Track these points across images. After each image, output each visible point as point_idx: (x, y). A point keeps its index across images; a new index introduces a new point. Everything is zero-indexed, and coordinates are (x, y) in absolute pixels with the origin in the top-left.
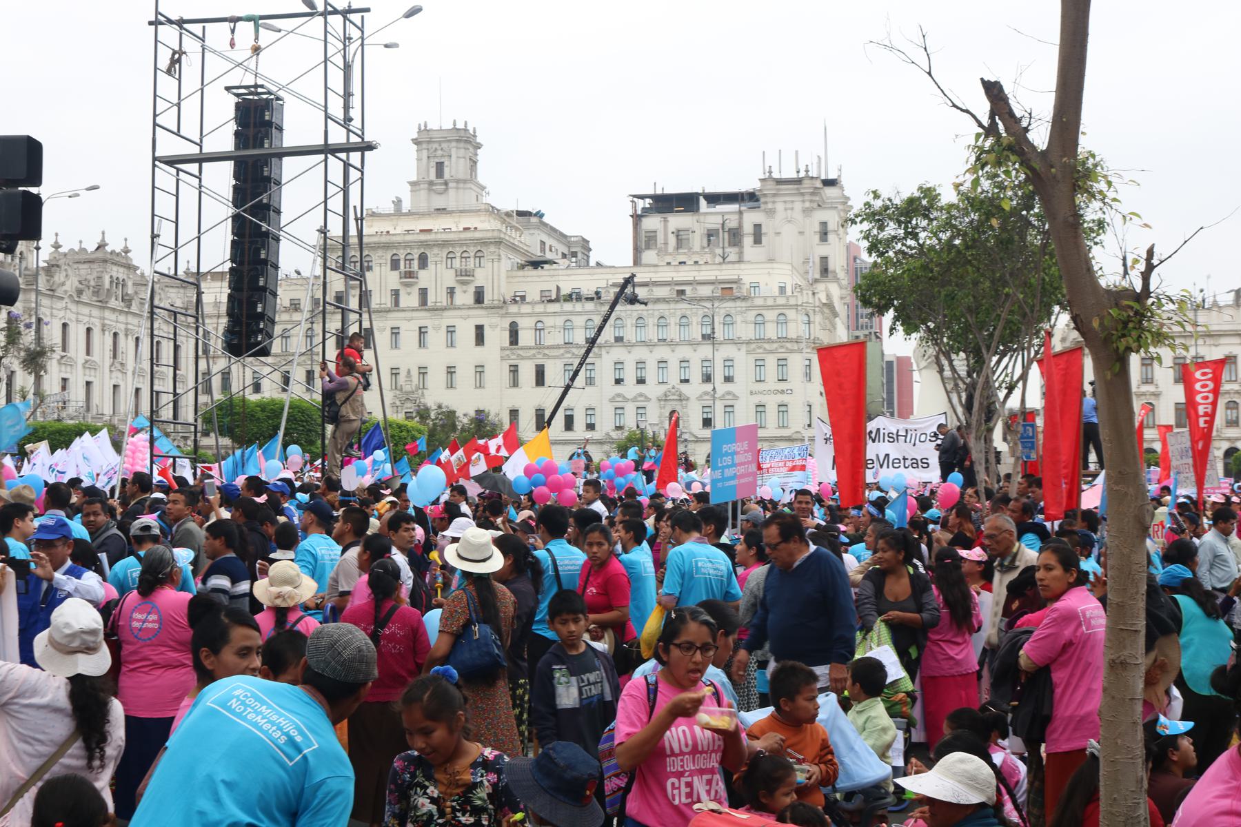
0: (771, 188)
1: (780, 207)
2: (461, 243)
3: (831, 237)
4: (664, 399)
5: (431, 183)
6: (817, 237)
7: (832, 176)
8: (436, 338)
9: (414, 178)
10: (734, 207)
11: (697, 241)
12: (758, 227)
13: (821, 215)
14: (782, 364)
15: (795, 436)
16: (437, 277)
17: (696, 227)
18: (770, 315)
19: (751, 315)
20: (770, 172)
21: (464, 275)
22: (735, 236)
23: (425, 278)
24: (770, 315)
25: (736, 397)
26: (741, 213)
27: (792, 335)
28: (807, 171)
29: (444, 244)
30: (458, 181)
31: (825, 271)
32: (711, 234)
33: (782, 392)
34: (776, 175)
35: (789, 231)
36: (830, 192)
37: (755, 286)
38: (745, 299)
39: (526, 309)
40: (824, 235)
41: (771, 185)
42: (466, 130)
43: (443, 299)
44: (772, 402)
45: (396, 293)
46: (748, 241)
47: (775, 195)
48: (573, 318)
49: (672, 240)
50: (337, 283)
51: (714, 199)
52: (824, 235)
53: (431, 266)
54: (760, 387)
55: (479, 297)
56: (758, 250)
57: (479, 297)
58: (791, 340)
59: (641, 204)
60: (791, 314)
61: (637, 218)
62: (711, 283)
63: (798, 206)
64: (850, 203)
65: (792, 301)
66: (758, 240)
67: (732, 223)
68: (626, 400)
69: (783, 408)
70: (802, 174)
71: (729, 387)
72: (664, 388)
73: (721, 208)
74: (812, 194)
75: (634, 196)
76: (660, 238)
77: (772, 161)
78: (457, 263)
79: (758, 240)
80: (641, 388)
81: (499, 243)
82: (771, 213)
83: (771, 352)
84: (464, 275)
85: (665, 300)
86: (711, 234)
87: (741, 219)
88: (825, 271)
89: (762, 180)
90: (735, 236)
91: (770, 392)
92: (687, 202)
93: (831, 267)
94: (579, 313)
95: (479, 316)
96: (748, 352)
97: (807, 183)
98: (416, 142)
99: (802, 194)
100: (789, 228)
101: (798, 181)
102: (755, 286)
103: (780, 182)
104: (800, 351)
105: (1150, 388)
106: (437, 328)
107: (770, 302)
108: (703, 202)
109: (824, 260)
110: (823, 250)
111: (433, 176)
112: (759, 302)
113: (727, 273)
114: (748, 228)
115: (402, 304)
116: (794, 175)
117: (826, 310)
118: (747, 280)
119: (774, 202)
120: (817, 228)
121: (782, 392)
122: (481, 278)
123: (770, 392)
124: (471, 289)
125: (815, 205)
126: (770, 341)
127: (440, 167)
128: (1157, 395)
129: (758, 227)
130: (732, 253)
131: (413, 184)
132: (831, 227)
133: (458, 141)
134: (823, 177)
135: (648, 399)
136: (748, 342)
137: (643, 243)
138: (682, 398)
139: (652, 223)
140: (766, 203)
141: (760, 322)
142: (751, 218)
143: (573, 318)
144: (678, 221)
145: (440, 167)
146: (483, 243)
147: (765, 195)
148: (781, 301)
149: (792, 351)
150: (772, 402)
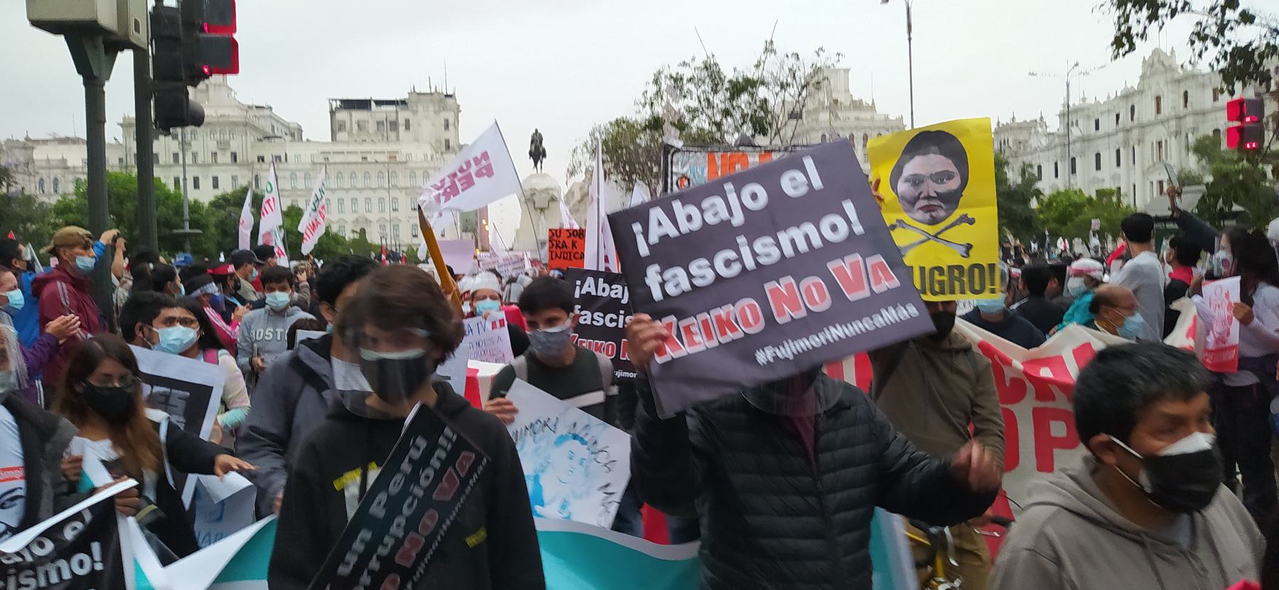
0: (414, 97)
1: (420, 109)
2: (219, 124)
3: (451, 127)
4: (357, 221)
7: (450, 93)
10: (392, 108)
11: (372, 127)
12: (407, 122)
13: (445, 115)
21: (223, 145)
22: (394, 125)
31: (448, 147)
32: (379, 123)
34: (417, 90)
36: (449, 101)
37: (409, 155)
40: (447, 126)
45: (176, 156)
46: (402, 128)
49: (355, 126)
51: (379, 103)
52: (447, 126)
55: (234, 157)
56: (407, 133)
57: (234, 157)
61: (332, 113)
63: (431, 109)
66: (407, 127)
67: (393, 118)
71: (394, 214)
73: (384, 108)
76: (348, 125)
78: (217, 137)
79: (407, 127)
80: (342, 216)
81: (246, 124)
82: (415, 112)
84: (223, 145)
85: (356, 163)
86: (379, 123)
88: (448, 147)
90: (394, 125)
92: (363, 105)
95: (235, 170)
100: (426, 123)
102: (409, 155)
106: (206, 177)
109: (447, 142)
110: (447, 135)
112: (411, 165)
113: (392, 147)
114: (401, 121)
118: (404, 152)
122: (235, 145)
129: (407, 122)
130: (392, 135)
132: (451, 121)
137: (337, 128)
138: (367, 221)
139: (343, 115)
141: (413, 175)
142: (403, 115)
144: (358, 115)
146: (235, 124)
148: (426, 165)
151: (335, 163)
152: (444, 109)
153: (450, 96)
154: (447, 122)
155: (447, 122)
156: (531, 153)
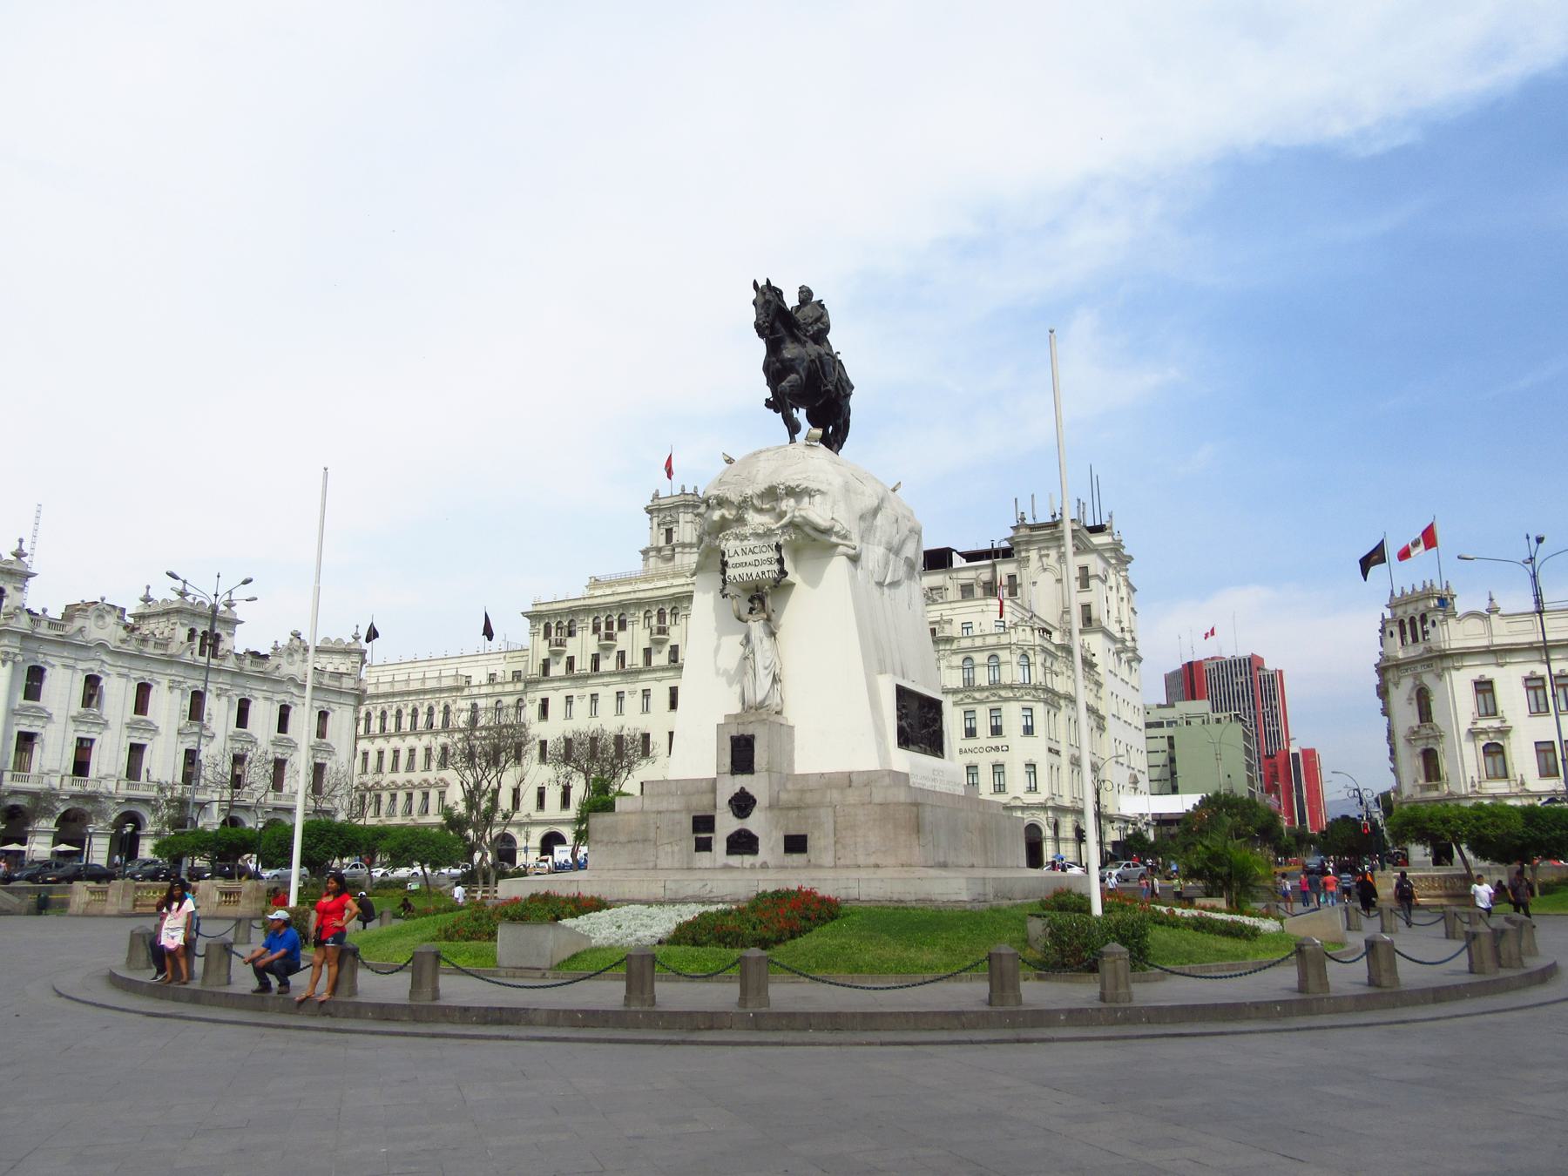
1: (1034, 555)
3: (1093, 583)
5: (659, 550)
6: (1076, 585)
8: (633, 703)
9: (647, 544)
11: (953, 593)
12: (1012, 577)
14: (995, 713)
16: (633, 640)
17: (949, 584)
18: (981, 658)
19: (957, 660)
20: (1023, 519)
23: (622, 640)
24: (981, 658)
26: (994, 566)
27: (1006, 680)
29: (638, 604)
30: (684, 545)
31: (1088, 619)
33: (997, 749)
34: (1029, 521)
36: (1097, 539)
37: (967, 626)
41: (1024, 532)
42: (695, 494)
43: (639, 662)
44: (985, 762)
47: (1028, 543)
50: (543, 649)
51: (971, 556)
52: (1085, 578)
53: (629, 627)
54: (971, 743)
58: (1005, 687)
60: (1004, 655)
64: (1125, 552)
65: (1004, 640)
66: (1013, 593)
69: (998, 768)
77: (1025, 507)
79: (1013, 593)
83: (981, 702)
87: (994, 571)
91: (981, 750)
93: (1094, 615)
96: (955, 704)
98: (649, 511)
102: (967, 626)
103: (1033, 528)
104: (1016, 699)
105: (1495, 723)
107: (978, 642)
108: (958, 561)
109: (1086, 608)
110: (1085, 597)
111: (662, 543)
112: (966, 643)
115: (602, 668)
116: (1050, 520)
119: (1027, 550)
121: (997, 749)
123: (981, 750)
124: (667, 649)
126: (981, 689)
127: (669, 532)
128: (1504, 732)
131: (645, 553)
132: (1091, 572)
133: (686, 506)
134: (1090, 524)
142: (1005, 569)
145: (669, 532)
147: (1018, 543)
148: (991, 641)
149: (1007, 700)
150: (985, 762)
153: (1098, 529)
154: (1084, 569)
155: (1084, 569)
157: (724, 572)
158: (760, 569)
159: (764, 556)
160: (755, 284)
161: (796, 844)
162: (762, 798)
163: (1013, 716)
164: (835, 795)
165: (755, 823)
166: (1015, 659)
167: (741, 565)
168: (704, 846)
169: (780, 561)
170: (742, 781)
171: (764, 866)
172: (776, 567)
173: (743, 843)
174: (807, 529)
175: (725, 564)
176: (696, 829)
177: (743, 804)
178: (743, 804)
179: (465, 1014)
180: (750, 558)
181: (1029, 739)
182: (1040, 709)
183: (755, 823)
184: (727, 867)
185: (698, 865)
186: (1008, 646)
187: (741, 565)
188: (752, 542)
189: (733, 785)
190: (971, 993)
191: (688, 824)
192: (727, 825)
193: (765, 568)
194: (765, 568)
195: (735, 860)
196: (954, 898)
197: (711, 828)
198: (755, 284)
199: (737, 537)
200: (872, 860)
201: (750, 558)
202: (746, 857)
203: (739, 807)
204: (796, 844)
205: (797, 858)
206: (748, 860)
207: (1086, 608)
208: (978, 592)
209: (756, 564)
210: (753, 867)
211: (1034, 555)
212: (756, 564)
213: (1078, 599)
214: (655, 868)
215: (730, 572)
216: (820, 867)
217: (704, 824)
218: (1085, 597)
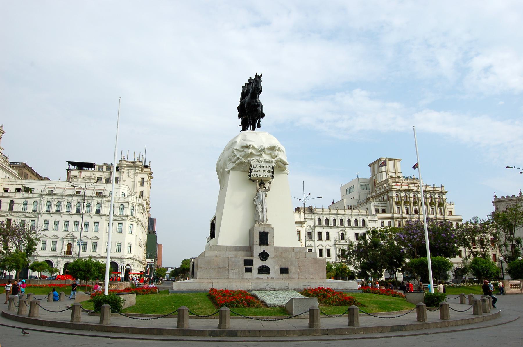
3: (145, 184)
15: (123, 257)
20: (124, 158)
25: (98, 238)
28: (138, 159)
34: (126, 159)
35: (129, 181)
36: (146, 170)
38: (106, 197)
39: (6, 194)
41: (124, 163)
47: (125, 167)
48: (28, 200)
59: (72, 167)
60: (126, 205)
62: (93, 190)
64: (152, 175)
65: (127, 200)
68: (47, 237)
70: (136, 160)
71: (96, 234)
72: (66, 233)
74: (139, 167)
75: (69, 162)
77: (125, 154)
86: (99, 179)
87: (111, 174)
89: (121, 161)
90: (108, 180)
94: (31, 198)
96: (106, 220)
97: (138, 163)
99: (135, 167)
101: (135, 162)
103: (127, 162)
109: (142, 192)
110: (142, 188)
117: (141, 207)
120: (140, 180)
125: (140, 172)
132: (145, 180)
135: (58, 237)
136: (107, 216)
138: (73, 238)
140: (121, 169)
143: (28, 200)
147: (121, 166)
149: (126, 220)
151: (56, 195)
152: (142, 172)
153: (146, 167)
154: (143, 179)
155: (143, 179)
156: (241, 108)
157: (251, 173)
158: (265, 174)
159: (267, 170)
160: (257, 74)
161: (284, 271)
162: (271, 255)
163: (127, 225)
164: (293, 255)
165: (268, 263)
166: (130, 207)
167: (258, 171)
168: (248, 270)
169: (273, 172)
170: (263, 248)
171: (272, 278)
172: (271, 174)
173: (264, 270)
174: (280, 163)
175: (251, 170)
176: (245, 265)
177: (264, 256)
178: (264, 256)
179: (366, 330)
180: (261, 169)
181: (131, 235)
182: (135, 224)
183: (268, 263)
184: (258, 278)
185: (246, 277)
186: (128, 202)
187: (258, 171)
188: (263, 164)
189: (258, 249)
190: (171, 323)
191: (242, 262)
192: (257, 263)
193: (267, 174)
194: (267, 174)
195: (261, 276)
196: (354, 288)
197: (252, 265)
198: (257, 74)
199: (258, 161)
200: (311, 276)
201: (261, 169)
202: (265, 275)
203: (263, 257)
204: (284, 271)
205: (284, 276)
206: (266, 276)
207: (142, 192)
208: (104, 181)
209: (263, 172)
210: (268, 278)
211: (126, 171)
212: (263, 172)
213: (139, 188)
214: (228, 278)
215: (253, 173)
216: (293, 279)
217: (248, 263)
218: (142, 188)
